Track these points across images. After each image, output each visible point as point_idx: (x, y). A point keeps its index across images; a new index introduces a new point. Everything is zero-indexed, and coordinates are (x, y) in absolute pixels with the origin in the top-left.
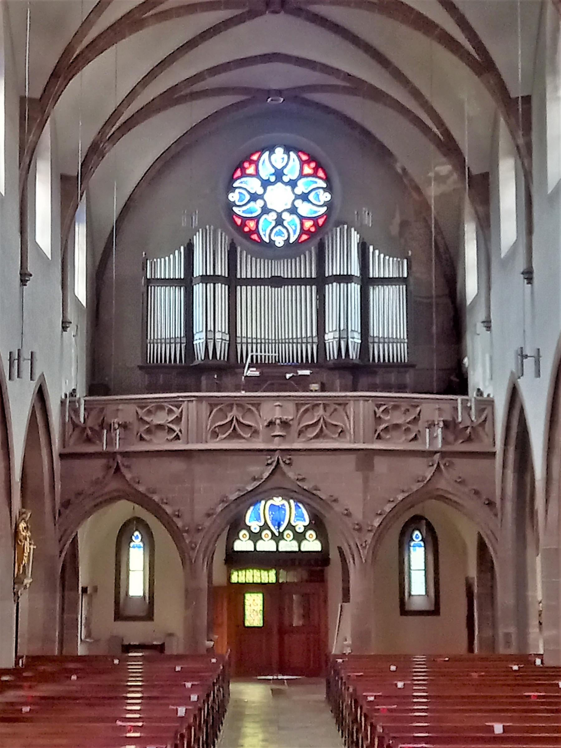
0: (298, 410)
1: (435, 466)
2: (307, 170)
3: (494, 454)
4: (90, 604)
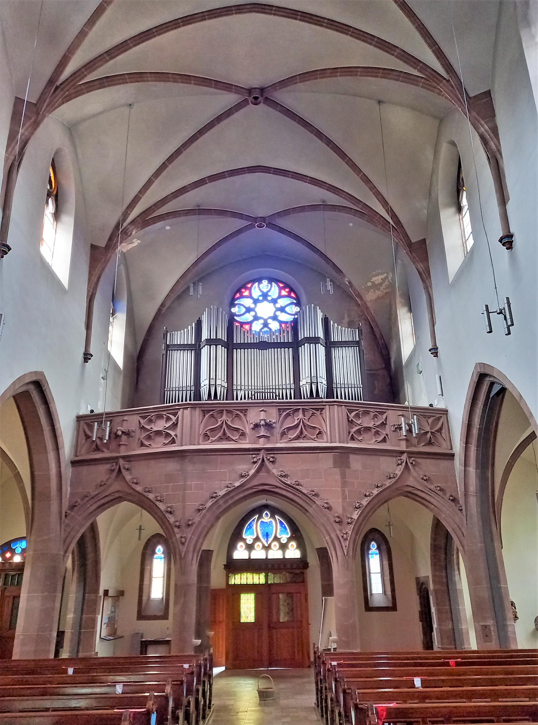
0: (280, 415)
1: (404, 464)
2: (284, 293)
3: (453, 455)
4: (115, 606)
